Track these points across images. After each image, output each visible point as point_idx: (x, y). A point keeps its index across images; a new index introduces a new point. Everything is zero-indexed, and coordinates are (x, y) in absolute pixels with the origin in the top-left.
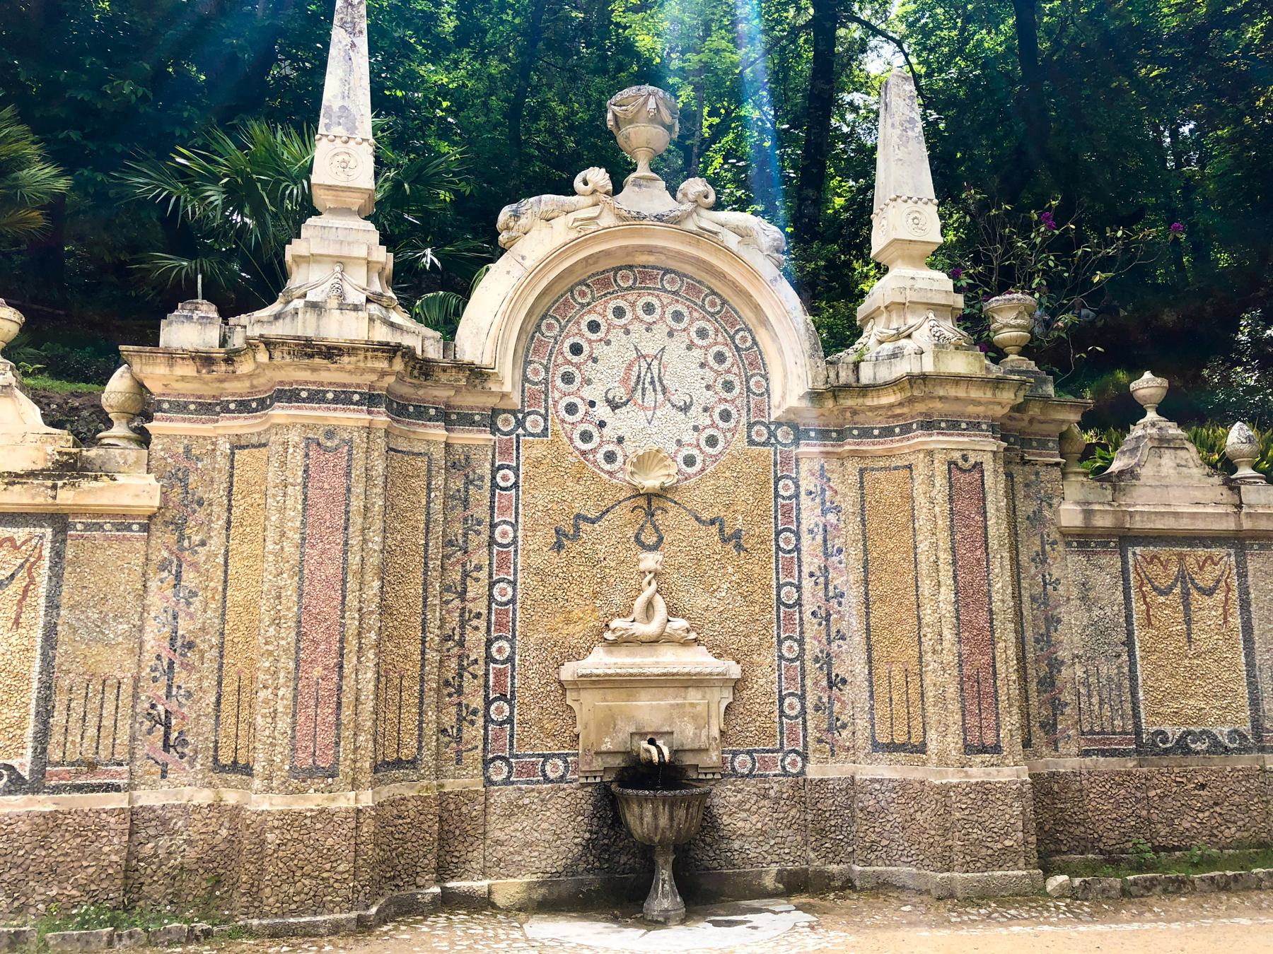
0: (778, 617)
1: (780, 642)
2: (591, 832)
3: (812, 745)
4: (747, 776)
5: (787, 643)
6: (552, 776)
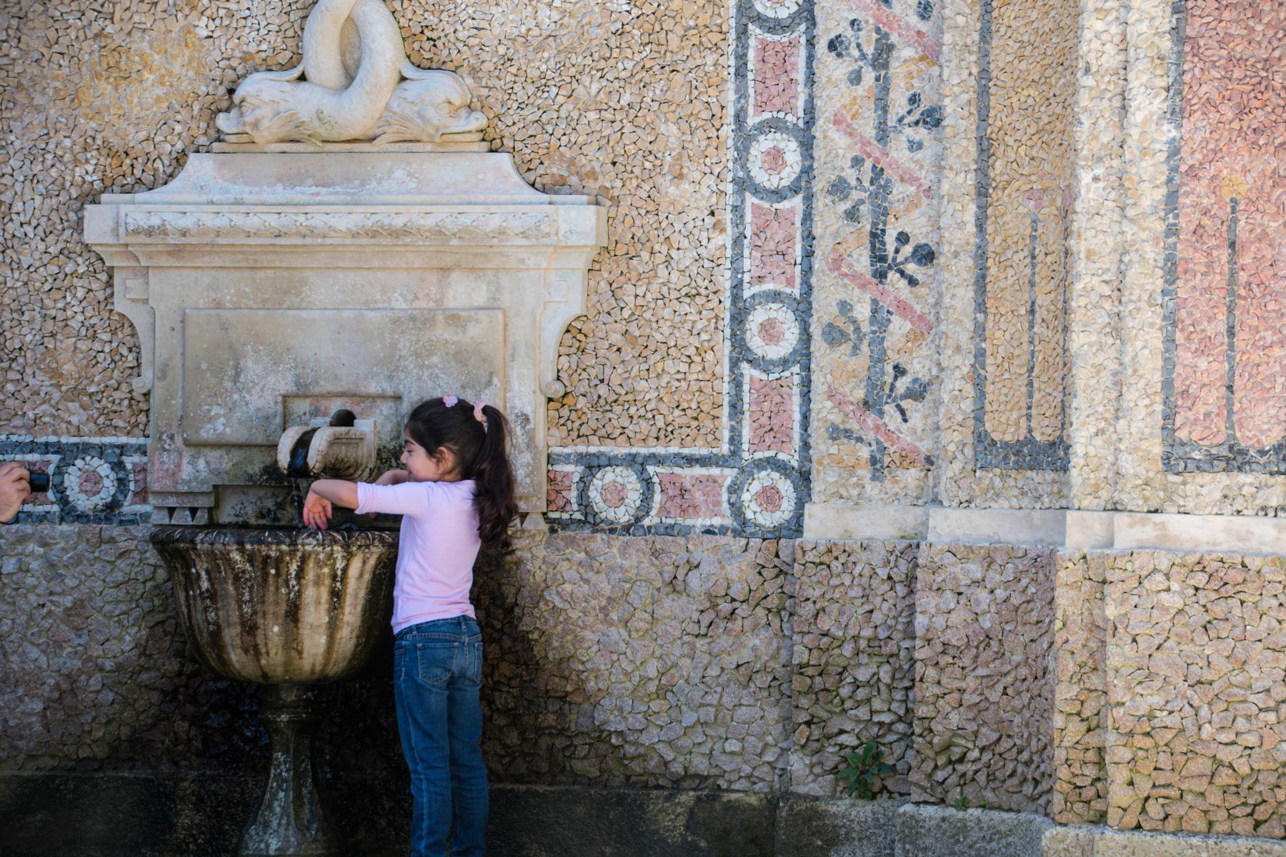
0: (741, 58)
1: (744, 139)
2: (179, 654)
3: (821, 446)
4: (627, 529)
5: (764, 143)
6: (84, 503)
